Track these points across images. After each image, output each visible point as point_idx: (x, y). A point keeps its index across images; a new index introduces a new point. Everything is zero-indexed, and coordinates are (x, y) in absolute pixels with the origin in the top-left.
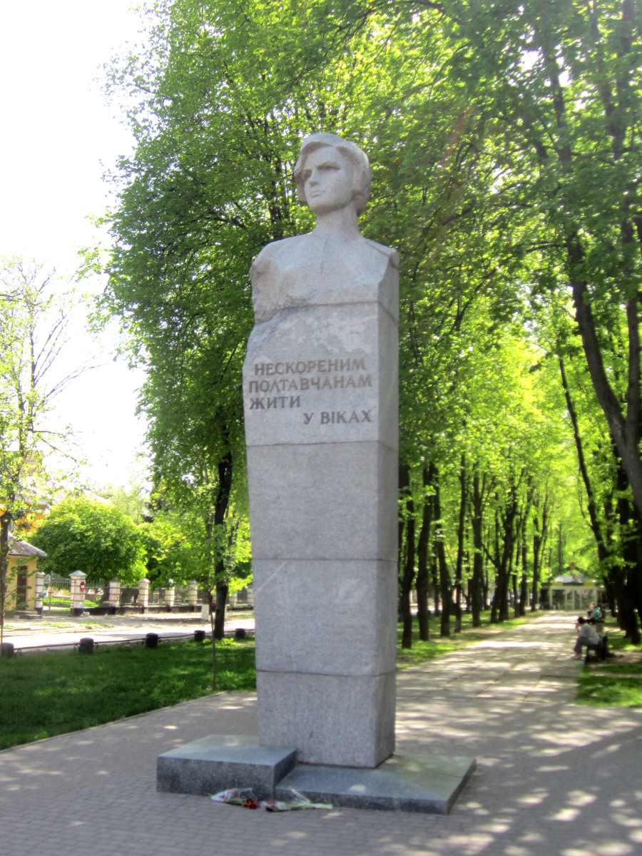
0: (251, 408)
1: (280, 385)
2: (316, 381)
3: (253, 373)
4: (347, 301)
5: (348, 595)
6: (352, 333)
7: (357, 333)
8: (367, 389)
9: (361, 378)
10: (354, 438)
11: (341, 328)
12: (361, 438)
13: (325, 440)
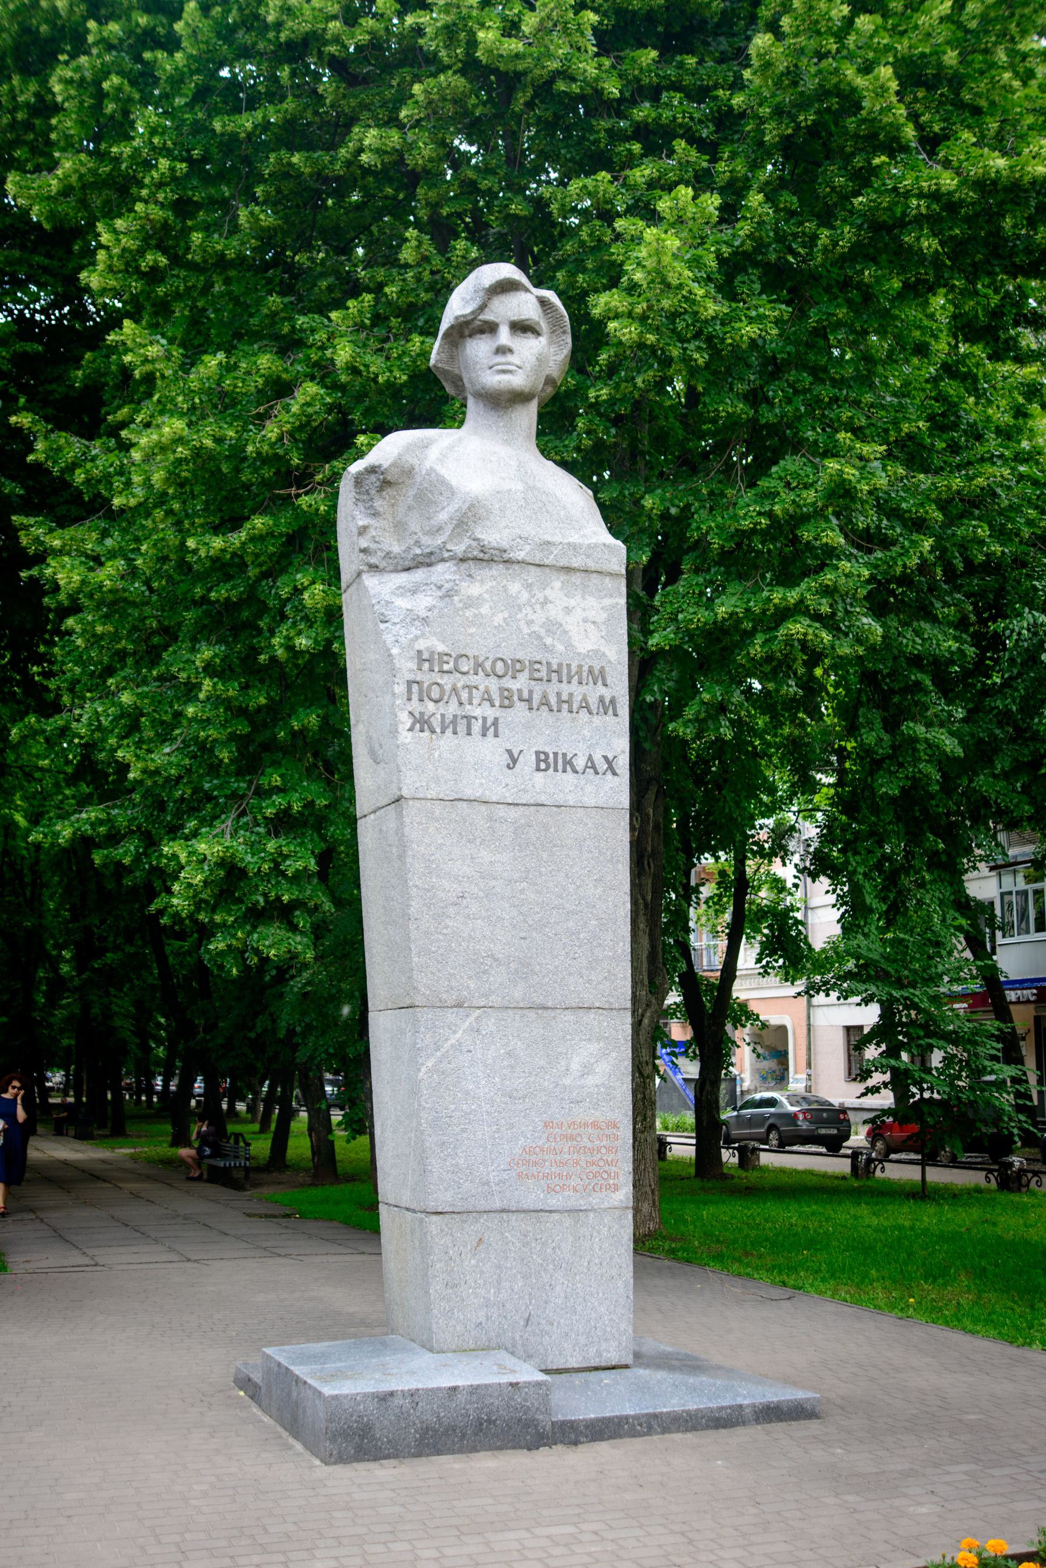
0: (411, 729)
1: (465, 695)
2: (526, 695)
3: (413, 665)
4: (576, 565)
5: (587, 1070)
6: (585, 621)
7: (594, 623)
8: (609, 718)
9: (601, 700)
11: (568, 610)
12: (601, 804)
13: (542, 799)
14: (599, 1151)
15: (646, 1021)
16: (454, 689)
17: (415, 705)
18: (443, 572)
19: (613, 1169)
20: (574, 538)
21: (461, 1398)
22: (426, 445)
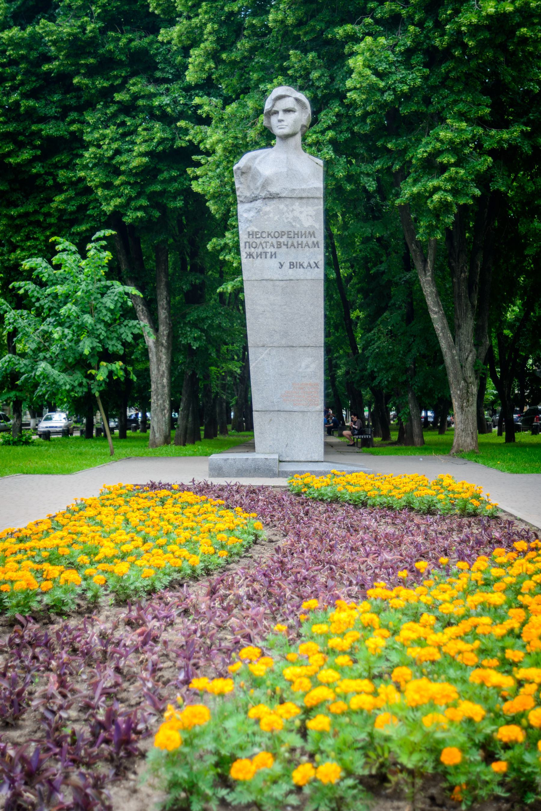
1: (264, 245)
3: (246, 236)
5: (307, 367)
8: (316, 249)
10: (309, 277)
11: (301, 212)
13: (292, 278)
15: (470, 358)
16: (261, 243)
17: (247, 250)
18: (258, 203)
20: (304, 186)
21: (250, 461)
22: (255, 158)
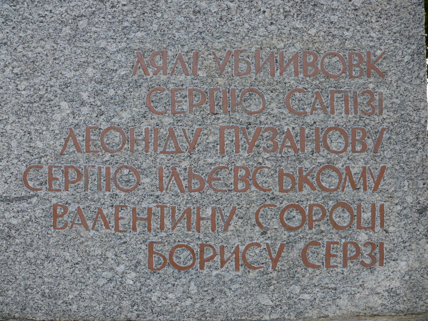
14: (321, 142)
19: (368, 197)
